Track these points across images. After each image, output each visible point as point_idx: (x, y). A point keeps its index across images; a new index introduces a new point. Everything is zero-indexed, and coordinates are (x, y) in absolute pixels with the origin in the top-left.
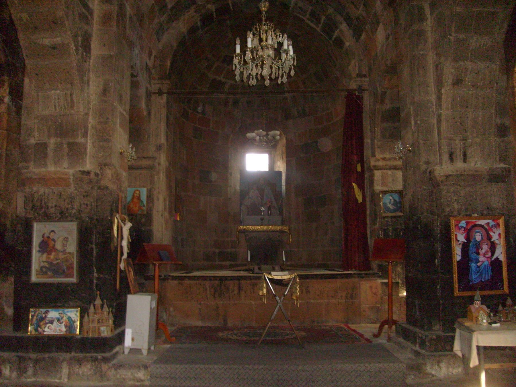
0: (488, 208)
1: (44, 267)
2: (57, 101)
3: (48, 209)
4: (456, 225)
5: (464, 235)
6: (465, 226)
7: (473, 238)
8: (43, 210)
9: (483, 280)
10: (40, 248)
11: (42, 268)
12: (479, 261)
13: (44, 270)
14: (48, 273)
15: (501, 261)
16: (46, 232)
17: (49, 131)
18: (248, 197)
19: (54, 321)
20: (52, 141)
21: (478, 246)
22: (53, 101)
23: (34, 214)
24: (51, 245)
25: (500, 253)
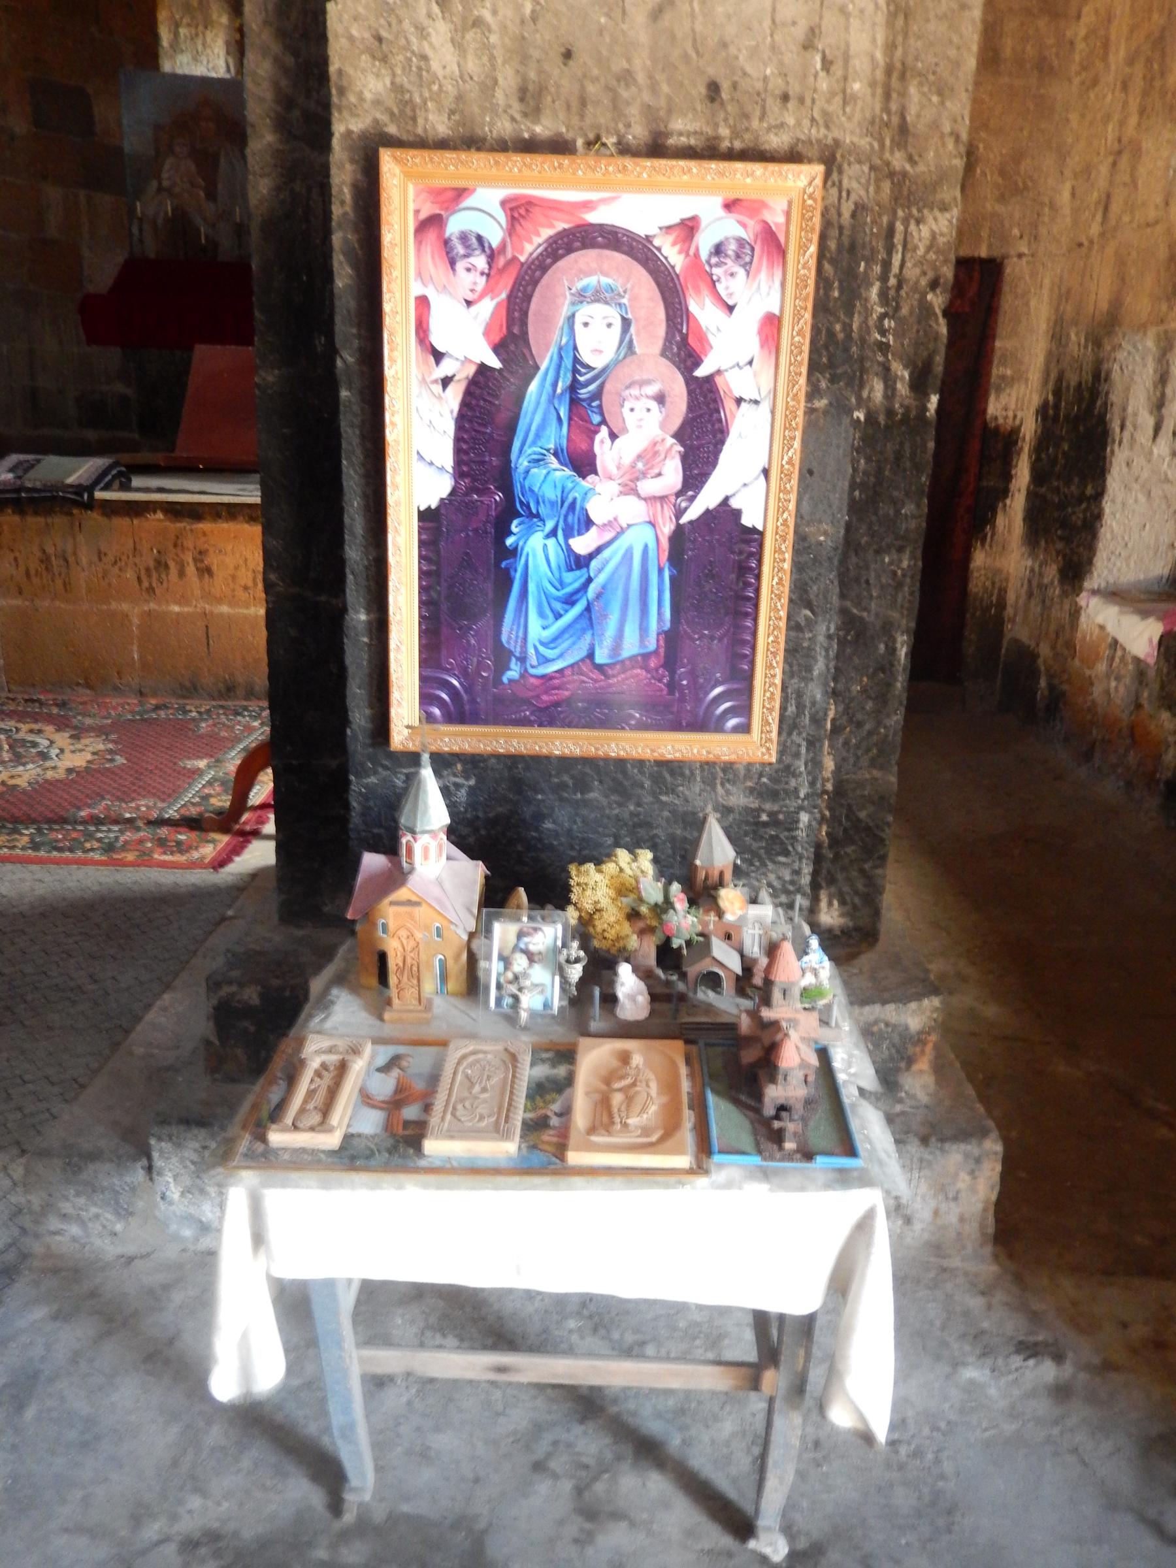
0: (714, 89)
4: (430, 224)
5: (487, 307)
6: (495, 236)
7: (558, 337)
9: (601, 657)
12: (588, 523)
15: (754, 537)
18: (155, 183)
21: (585, 406)
25: (752, 476)
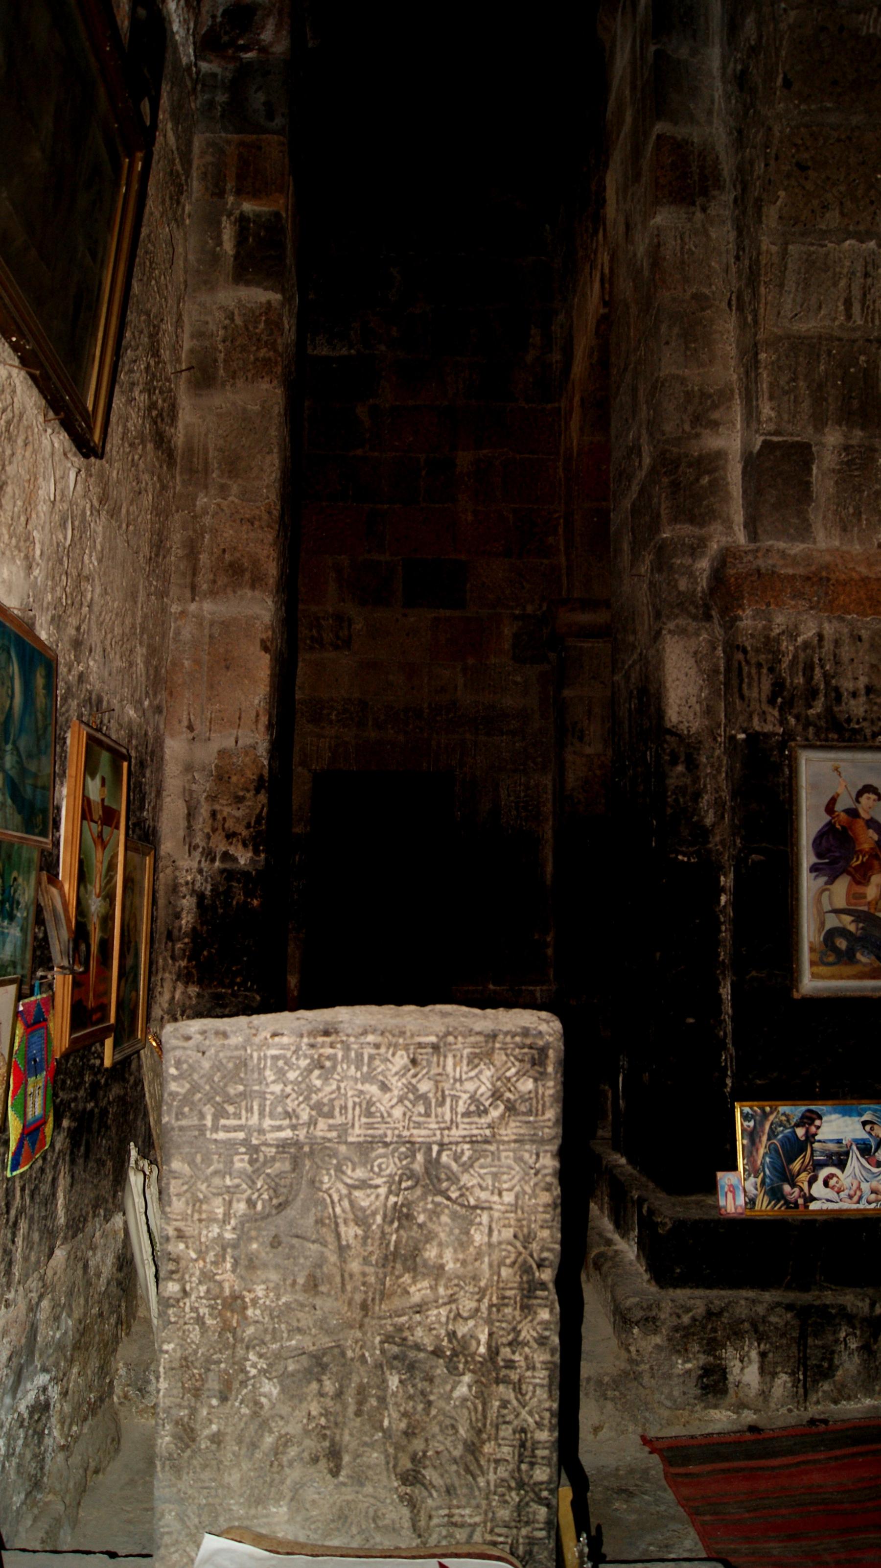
1: (842, 932)
2: (858, 281)
3: (839, 699)
8: (818, 707)
10: (819, 855)
11: (831, 936)
13: (842, 944)
14: (859, 956)
16: (840, 790)
17: (818, 399)
19: (847, 1154)
20: (833, 437)
22: (843, 283)
23: (783, 722)
24: (866, 847)
